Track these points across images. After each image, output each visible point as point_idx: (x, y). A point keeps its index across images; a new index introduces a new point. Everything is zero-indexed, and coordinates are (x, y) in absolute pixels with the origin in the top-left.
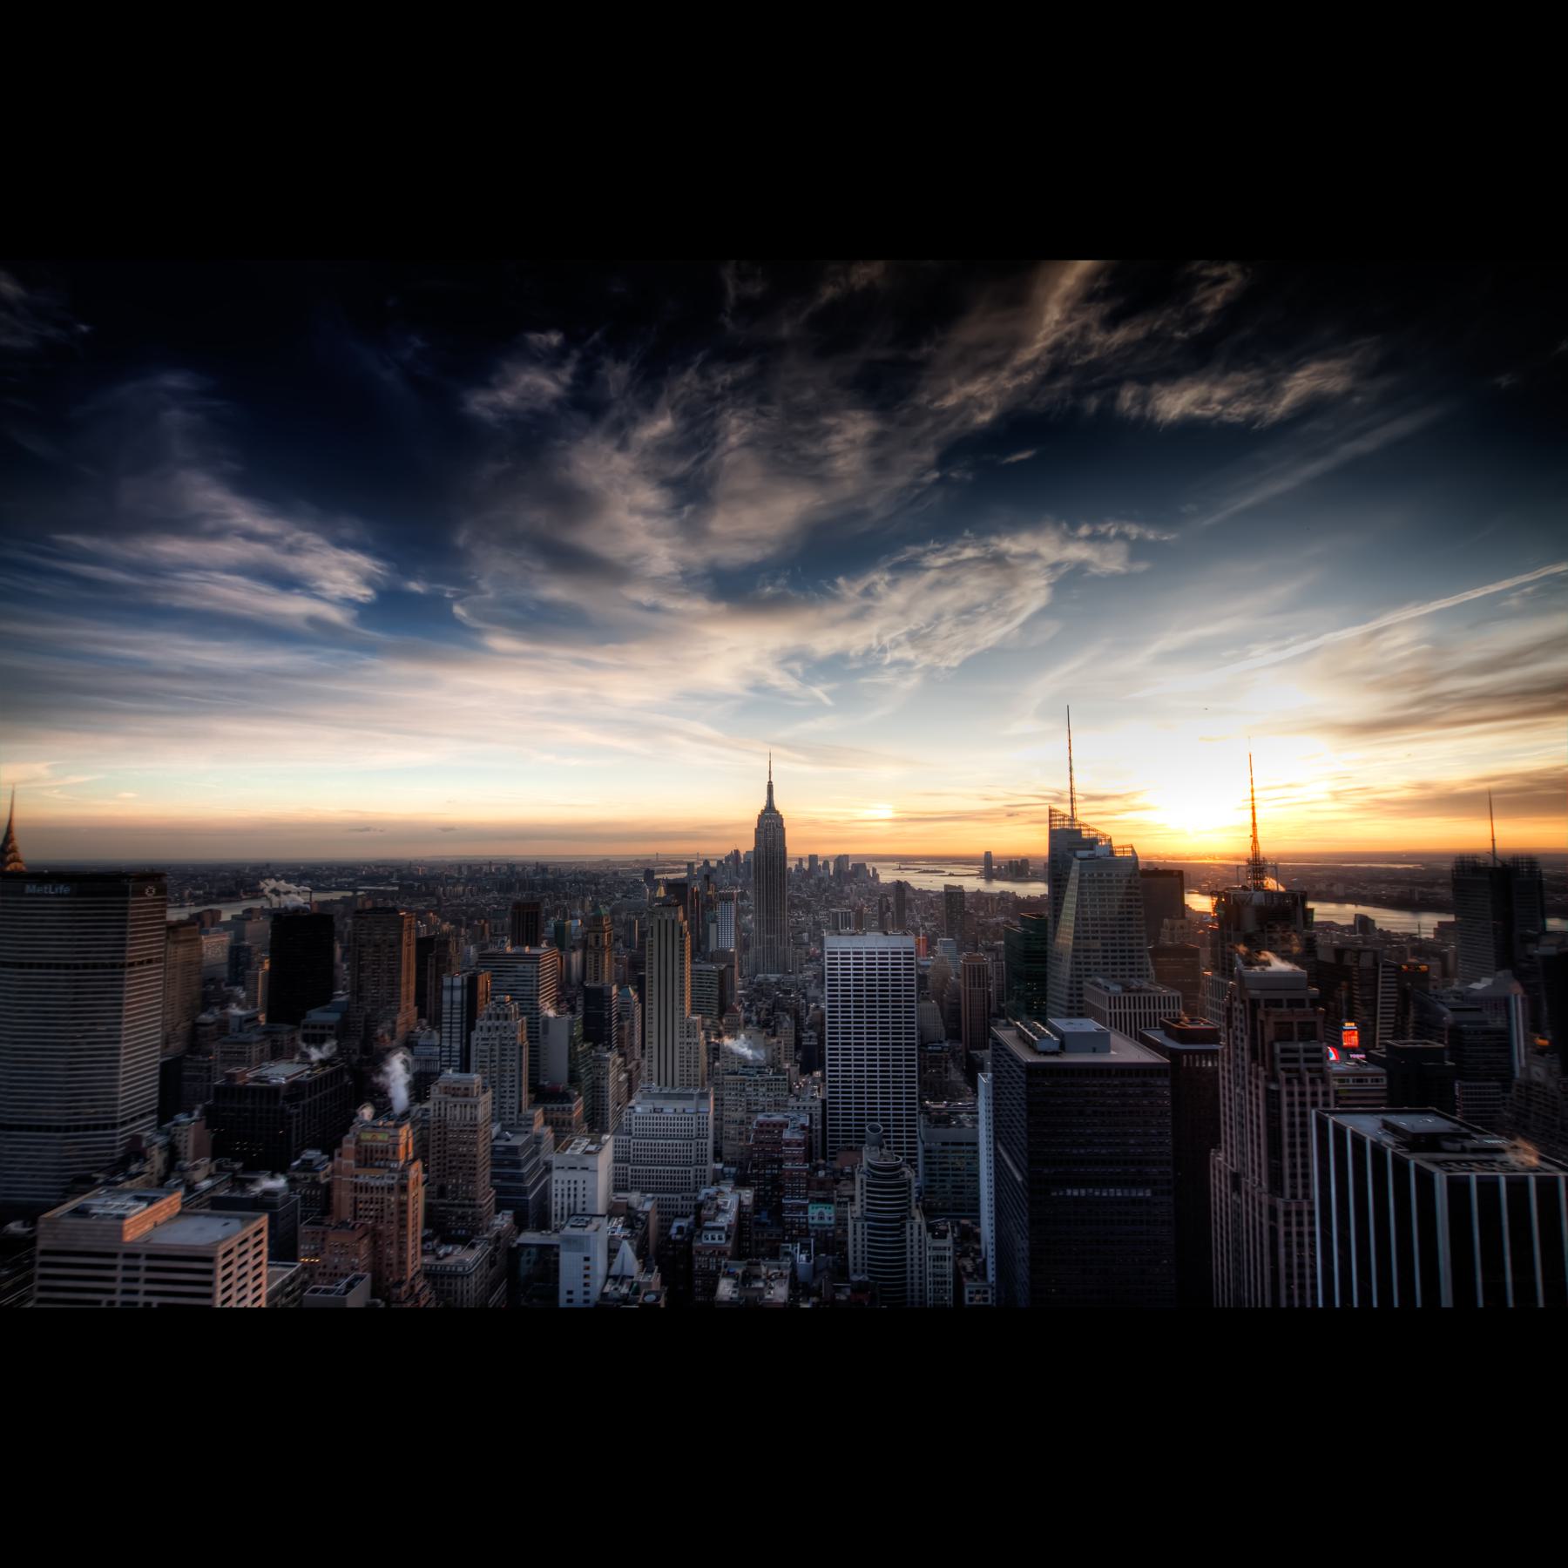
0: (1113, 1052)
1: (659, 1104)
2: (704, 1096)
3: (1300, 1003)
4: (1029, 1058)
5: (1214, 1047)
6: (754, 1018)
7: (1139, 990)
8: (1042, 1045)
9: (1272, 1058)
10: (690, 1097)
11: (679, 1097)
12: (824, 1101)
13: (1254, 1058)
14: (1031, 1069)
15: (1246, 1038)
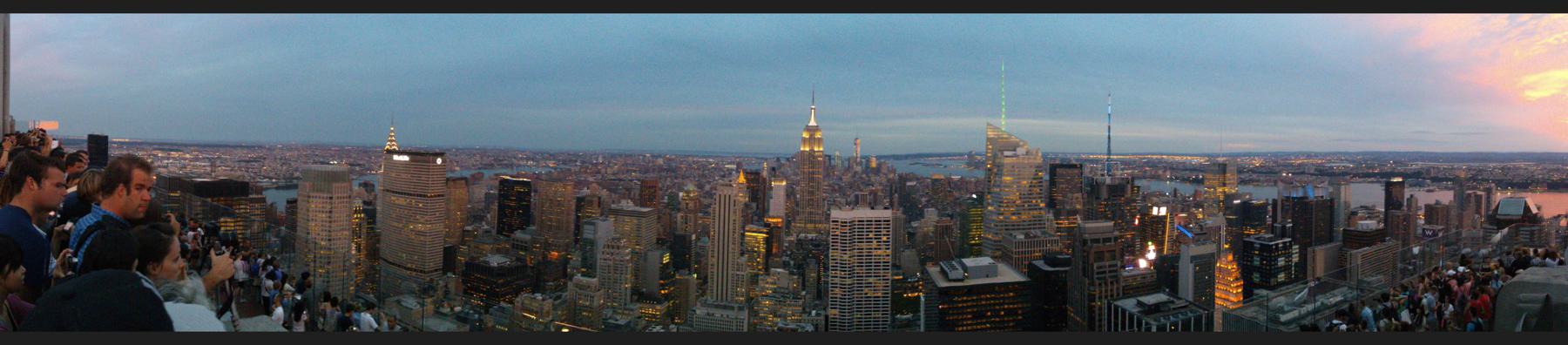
0: (999, 277)
1: (711, 311)
2: (741, 309)
3: (1108, 240)
4: (943, 284)
5: (1067, 269)
6: (792, 262)
7: (1035, 237)
8: (952, 275)
9: (1093, 274)
10: (732, 308)
11: (725, 307)
12: (827, 317)
13: (1084, 275)
14: (945, 292)
15: (1081, 263)
